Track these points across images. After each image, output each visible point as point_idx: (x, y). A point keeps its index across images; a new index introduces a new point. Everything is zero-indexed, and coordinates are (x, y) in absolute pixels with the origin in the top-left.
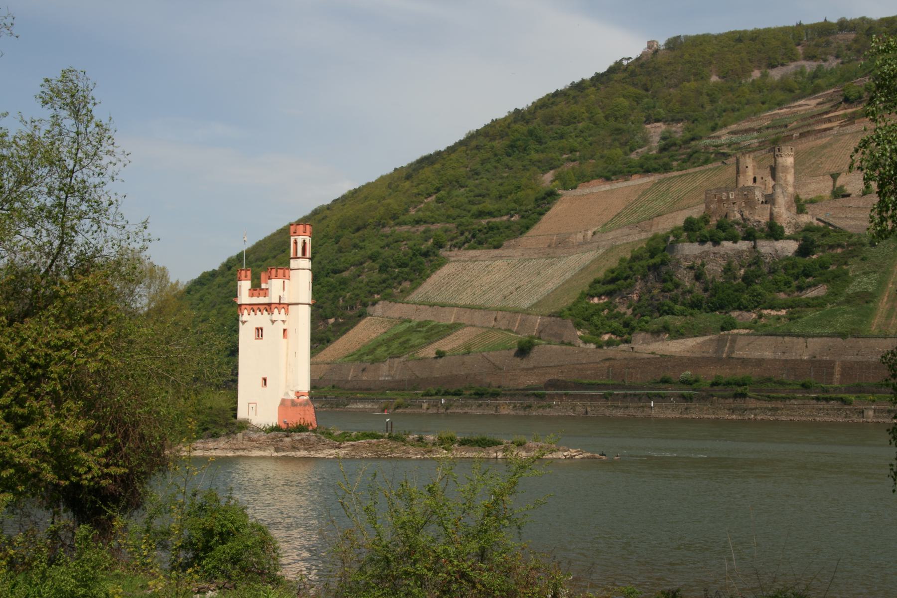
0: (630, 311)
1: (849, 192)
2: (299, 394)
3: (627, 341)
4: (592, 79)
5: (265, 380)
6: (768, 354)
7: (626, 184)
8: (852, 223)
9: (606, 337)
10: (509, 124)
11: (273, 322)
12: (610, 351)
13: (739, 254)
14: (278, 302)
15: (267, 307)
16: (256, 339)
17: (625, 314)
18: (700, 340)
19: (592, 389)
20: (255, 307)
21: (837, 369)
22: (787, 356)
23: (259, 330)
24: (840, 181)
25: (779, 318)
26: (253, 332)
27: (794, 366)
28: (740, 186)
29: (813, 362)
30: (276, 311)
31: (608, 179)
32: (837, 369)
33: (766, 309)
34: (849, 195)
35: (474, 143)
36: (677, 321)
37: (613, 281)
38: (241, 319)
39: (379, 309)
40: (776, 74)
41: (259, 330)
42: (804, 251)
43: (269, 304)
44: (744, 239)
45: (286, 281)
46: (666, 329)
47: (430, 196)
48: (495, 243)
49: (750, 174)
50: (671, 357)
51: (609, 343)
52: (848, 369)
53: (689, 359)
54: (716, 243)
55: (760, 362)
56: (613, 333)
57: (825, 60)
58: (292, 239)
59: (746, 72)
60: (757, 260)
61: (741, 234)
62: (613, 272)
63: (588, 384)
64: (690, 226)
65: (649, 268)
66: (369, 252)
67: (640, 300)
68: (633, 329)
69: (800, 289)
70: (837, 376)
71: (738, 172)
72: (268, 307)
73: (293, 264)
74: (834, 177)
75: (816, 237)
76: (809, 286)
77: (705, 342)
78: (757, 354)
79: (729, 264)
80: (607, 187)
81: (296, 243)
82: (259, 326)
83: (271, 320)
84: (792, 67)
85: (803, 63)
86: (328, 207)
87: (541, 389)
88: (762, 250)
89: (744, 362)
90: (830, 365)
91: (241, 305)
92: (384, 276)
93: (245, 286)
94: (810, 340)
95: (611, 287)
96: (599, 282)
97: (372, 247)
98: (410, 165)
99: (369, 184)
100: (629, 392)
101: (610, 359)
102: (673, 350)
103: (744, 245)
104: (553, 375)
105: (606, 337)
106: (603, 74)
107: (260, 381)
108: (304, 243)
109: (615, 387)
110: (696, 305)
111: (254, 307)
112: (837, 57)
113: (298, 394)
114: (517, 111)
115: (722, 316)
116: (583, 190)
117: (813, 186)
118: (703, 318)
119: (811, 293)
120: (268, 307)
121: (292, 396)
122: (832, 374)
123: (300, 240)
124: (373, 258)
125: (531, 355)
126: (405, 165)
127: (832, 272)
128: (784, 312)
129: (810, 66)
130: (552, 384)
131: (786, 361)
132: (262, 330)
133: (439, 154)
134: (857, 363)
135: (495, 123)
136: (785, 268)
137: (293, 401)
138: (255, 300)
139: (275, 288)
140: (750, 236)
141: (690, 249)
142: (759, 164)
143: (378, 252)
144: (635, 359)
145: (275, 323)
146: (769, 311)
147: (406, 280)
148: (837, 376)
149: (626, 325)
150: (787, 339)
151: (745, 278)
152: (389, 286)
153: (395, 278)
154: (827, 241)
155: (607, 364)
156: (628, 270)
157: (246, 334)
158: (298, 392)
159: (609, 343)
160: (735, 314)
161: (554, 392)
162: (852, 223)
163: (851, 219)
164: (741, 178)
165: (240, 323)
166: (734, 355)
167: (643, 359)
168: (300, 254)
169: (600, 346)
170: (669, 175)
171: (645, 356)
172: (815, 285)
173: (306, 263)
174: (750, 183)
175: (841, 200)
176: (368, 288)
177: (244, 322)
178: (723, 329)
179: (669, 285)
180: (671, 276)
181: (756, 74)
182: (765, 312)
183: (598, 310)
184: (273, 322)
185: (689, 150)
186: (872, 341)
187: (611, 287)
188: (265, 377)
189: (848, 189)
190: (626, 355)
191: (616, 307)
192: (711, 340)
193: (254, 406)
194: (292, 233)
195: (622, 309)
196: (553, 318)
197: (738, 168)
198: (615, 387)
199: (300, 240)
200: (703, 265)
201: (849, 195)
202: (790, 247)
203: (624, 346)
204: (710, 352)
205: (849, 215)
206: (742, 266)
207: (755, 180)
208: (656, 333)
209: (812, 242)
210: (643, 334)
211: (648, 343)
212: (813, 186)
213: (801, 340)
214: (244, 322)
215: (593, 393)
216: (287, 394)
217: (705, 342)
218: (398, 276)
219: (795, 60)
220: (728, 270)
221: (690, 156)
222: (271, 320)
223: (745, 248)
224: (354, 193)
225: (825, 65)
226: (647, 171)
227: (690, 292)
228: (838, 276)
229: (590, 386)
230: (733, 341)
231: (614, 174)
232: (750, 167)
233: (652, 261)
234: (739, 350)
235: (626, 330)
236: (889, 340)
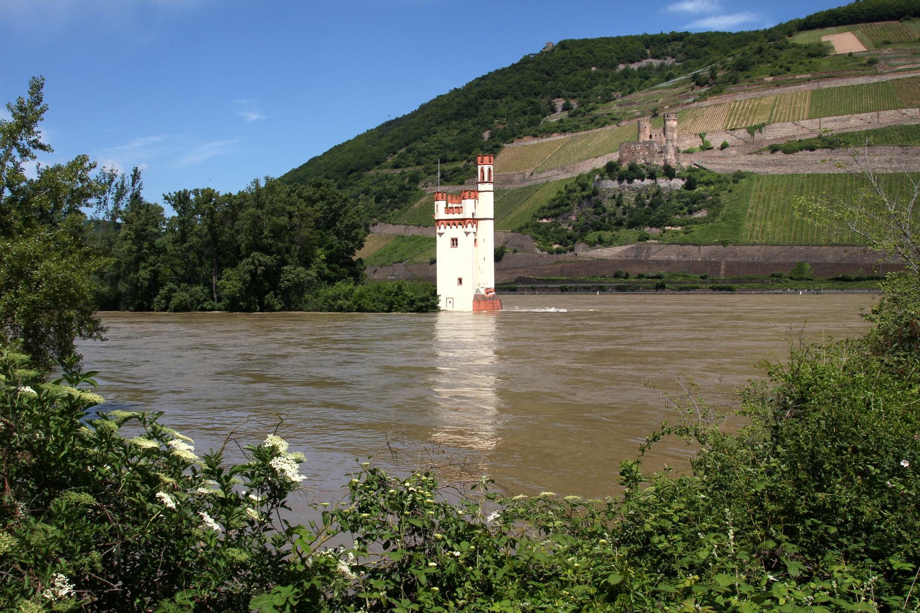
0: (571, 228)
1: (712, 146)
3: (572, 250)
4: (510, 67)
5: (460, 281)
6: (673, 257)
7: (549, 139)
8: (718, 167)
9: (555, 247)
10: (453, 99)
11: (467, 233)
12: (561, 257)
13: (645, 188)
14: (471, 217)
15: (462, 222)
17: (567, 230)
18: (624, 248)
19: (550, 283)
20: (451, 222)
21: (723, 267)
22: (686, 259)
23: (455, 242)
24: (706, 138)
25: (677, 232)
26: (449, 242)
27: (692, 265)
28: (641, 141)
29: (706, 263)
30: (469, 225)
31: (535, 136)
32: (723, 267)
33: (667, 226)
34: (712, 148)
35: (428, 112)
36: (607, 235)
37: (558, 206)
38: (438, 231)
39: (376, 230)
40: (635, 66)
41: (455, 242)
42: (690, 185)
43: (464, 220)
44: (649, 178)
46: (601, 241)
47: (401, 149)
48: (458, 181)
49: (648, 132)
50: (601, 262)
51: (558, 252)
52: (730, 267)
53: (619, 261)
54: (630, 181)
55: (669, 263)
56: (560, 244)
57: (665, 59)
58: (480, 167)
59: (614, 66)
60: (658, 193)
61: (647, 175)
62: (554, 200)
63: (547, 280)
64: (611, 168)
65: (584, 198)
66: (362, 189)
67: (578, 220)
68: (575, 241)
70: (722, 272)
71: (639, 131)
72: (463, 222)
74: (701, 136)
75: (695, 175)
76: (696, 211)
79: (639, 195)
80: (535, 142)
81: (482, 171)
82: (454, 237)
83: (465, 232)
84: (644, 63)
85: (651, 60)
86: (321, 158)
87: (511, 283)
88: (661, 185)
89: (658, 263)
90: (717, 264)
91: (438, 220)
92: (379, 205)
93: (440, 206)
94: (702, 247)
95: (557, 211)
96: (545, 208)
97: (364, 185)
98: (378, 128)
99: (349, 142)
100: (579, 285)
101: (562, 262)
102: (606, 255)
103: (647, 182)
104: (521, 274)
105: (555, 247)
106: (517, 65)
107: (457, 281)
108: (490, 171)
109: (568, 281)
110: (619, 224)
111: (450, 223)
112: (673, 57)
113: (488, 291)
114: (456, 89)
115: (638, 231)
116: (517, 145)
117: (688, 142)
118: (624, 232)
119: (698, 215)
120: (463, 222)
121: (483, 292)
122: (719, 271)
123: (486, 168)
124: (367, 192)
125: (503, 259)
126: (374, 128)
127: (710, 200)
128: (679, 228)
129: (656, 63)
130: (520, 280)
131: (688, 262)
132: (456, 240)
133: (397, 119)
134: (736, 262)
135: (440, 98)
136: (677, 197)
137: (483, 296)
139: (468, 207)
140: (652, 176)
141: (611, 185)
142: (653, 127)
143: (369, 188)
144: (580, 261)
145: (469, 235)
146: (670, 228)
147: (396, 207)
148: (722, 272)
149: (569, 238)
150: (686, 247)
151: (651, 205)
152: (384, 212)
153: (388, 207)
154: (704, 179)
155: (560, 265)
156: (566, 199)
157: (442, 245)
158: (487, 289)
159: (558, 252)
160: (647, 229)
161: (524, 286)
162: (718, 167)
163: (717, 164)
164: (642, 136)
166: (649, 259)
167: (586, 261)
168: (486, 179)
169: (551, 253)
170: (579, 133)
171: (587, 259)
172: (700, 209)
173: (490, 187)
174: (648, 139)
175: (708, 152)
176: (369, 214)
177: (441, 234)
178: (640, 240)
179: (600, 210)
180: (600, 203)
181: (621, 67)
182: (667, 228)
183: (548, 227)
184: (467, 233)
185: (590, 117)
186: (745, 247)
187: (557, 211)
189: (712, 144)
190: (573, 259)
191: (560, 225)
192: (632, 248)
193: (451, 300)
194: (479, 163)
195: (565, 226)
196: (515, 234)
197: (639, 128)
198: (568, 281)
199: (486, 168)
200: (621, 195)
201: (712, 148)
202: (678, 183)
203: (569, 254)
204: (632, 256)
205: (715, 162)
206: (648, 197)
207: (651, 136)
208: (592, 245)
209: (694, 180)
210: (583, 244)
211: (587, 251)
212: (688, 142)
213: (696, 248)
214: (441, 234)
215: (553, 286)
216: (478, 290)
217: (628, 249)
218: (389, 204)
219: (645, 59)
220: (638, 199)
221: (592, 121)
222: (465, 232)
223: (649, 183)
224: (338, 148)
225: (666, 62)
226: (564, 131)
227: (614, 214)
228: (714, 203)
229: (554, 281)
230: (649, 248)
232: (648, 128)
233: (584, 193)
234: (654, 254)
235: (568, 242)
236: (755, 247)
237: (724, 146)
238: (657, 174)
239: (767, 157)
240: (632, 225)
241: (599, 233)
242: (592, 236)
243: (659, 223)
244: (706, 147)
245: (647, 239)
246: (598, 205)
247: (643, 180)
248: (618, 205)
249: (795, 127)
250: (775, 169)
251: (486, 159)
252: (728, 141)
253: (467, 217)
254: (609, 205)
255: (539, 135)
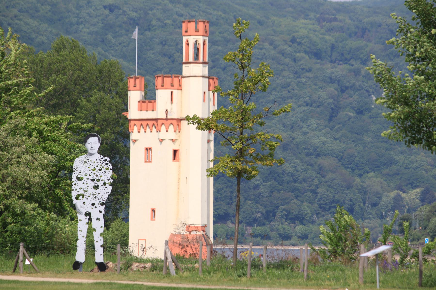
2: (190, 229)
5: (153, 211)
14: (164, 117)
16: (146, 162)
20: (144, 123)
30: (163, 128)
43: (156, 120)
45: (175, 92)
58: (185, 39)
73: (186, 70)
82: (148, 146)
91: (130, 120)
123: (192, 40)
132: (150, 149)
145: (163, 142)
165: (131, 142)
168: (191, 59)
184: (161, 141)
188: (153, 207)
194: (184, 33)
199: (192, 40)
251: (192, 25)
253: (159, 117)
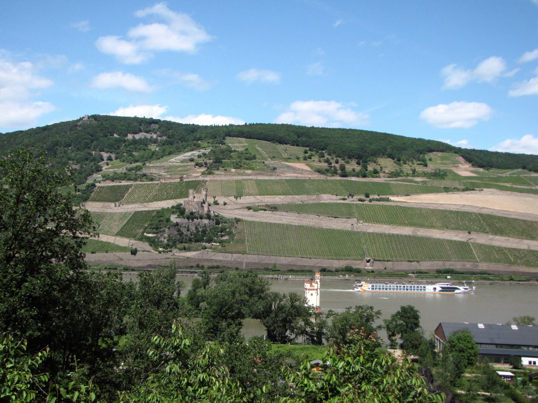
1: (219, 203)
6: (221, 258)
8: (226, 215)
17: (164, 241)
23: (312, 295)
31: (113, 181)
32: (244, 264)
41: (312, 295)
46: (184, 249)
52: (247, 264)
54: (193, 220)
55: (221, 261)
69: (222, 236)
72: (314, 290)
74: (214, 197)
76: (223, 236)
77: (198, 254)
78: (217, 258)
102: (188, 255)
110: (190, 240)
120: (314, 290)
138: (311, 288)
148: (244, 266)
150: (226, 254)
162: (226, 215)
182: (212, 243)
201: (219, 204)
213: (231, 254)
231: (115, 179)
237: (225, 204)
238: (203, 217)
239: (246, 212)
240: (196, 241)
241: (184, 244)
242: (179, 246)
243: (210, 241)
244: (216, 203)
245: (206, 248)
246: (179, 231)
247: (197, 219)
248: (188, 230)
249: (255, 199)
250: (251, 218)
252: (226, 201)
254: (184, 231)
255: (115, 180)
